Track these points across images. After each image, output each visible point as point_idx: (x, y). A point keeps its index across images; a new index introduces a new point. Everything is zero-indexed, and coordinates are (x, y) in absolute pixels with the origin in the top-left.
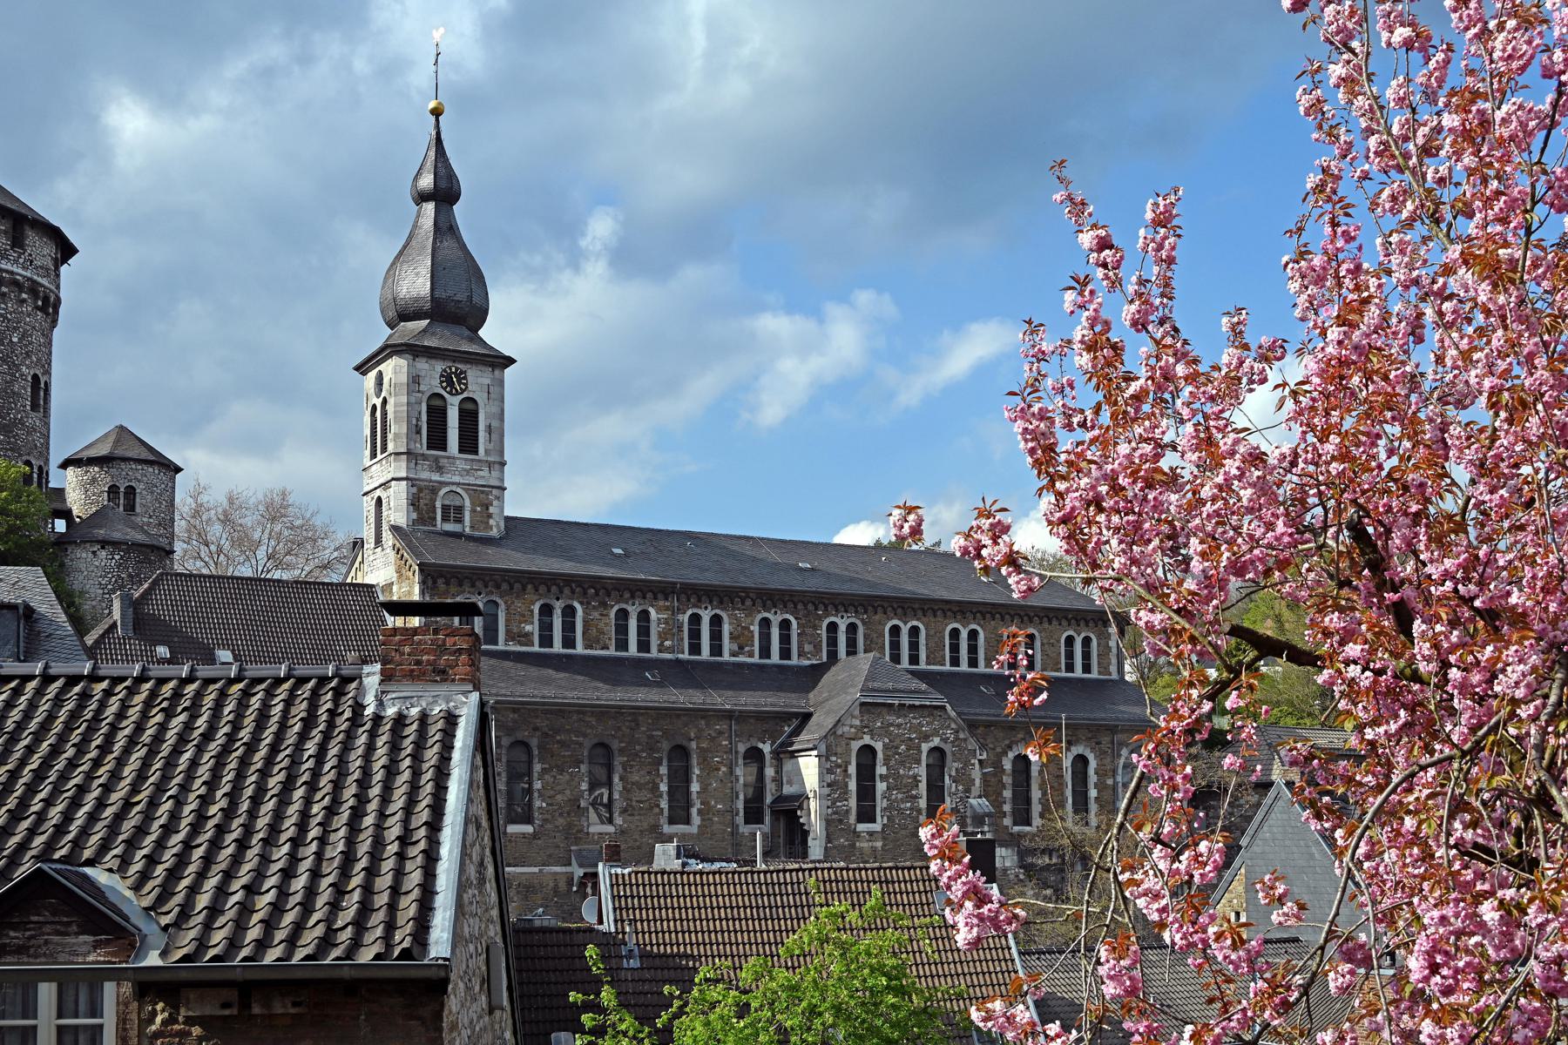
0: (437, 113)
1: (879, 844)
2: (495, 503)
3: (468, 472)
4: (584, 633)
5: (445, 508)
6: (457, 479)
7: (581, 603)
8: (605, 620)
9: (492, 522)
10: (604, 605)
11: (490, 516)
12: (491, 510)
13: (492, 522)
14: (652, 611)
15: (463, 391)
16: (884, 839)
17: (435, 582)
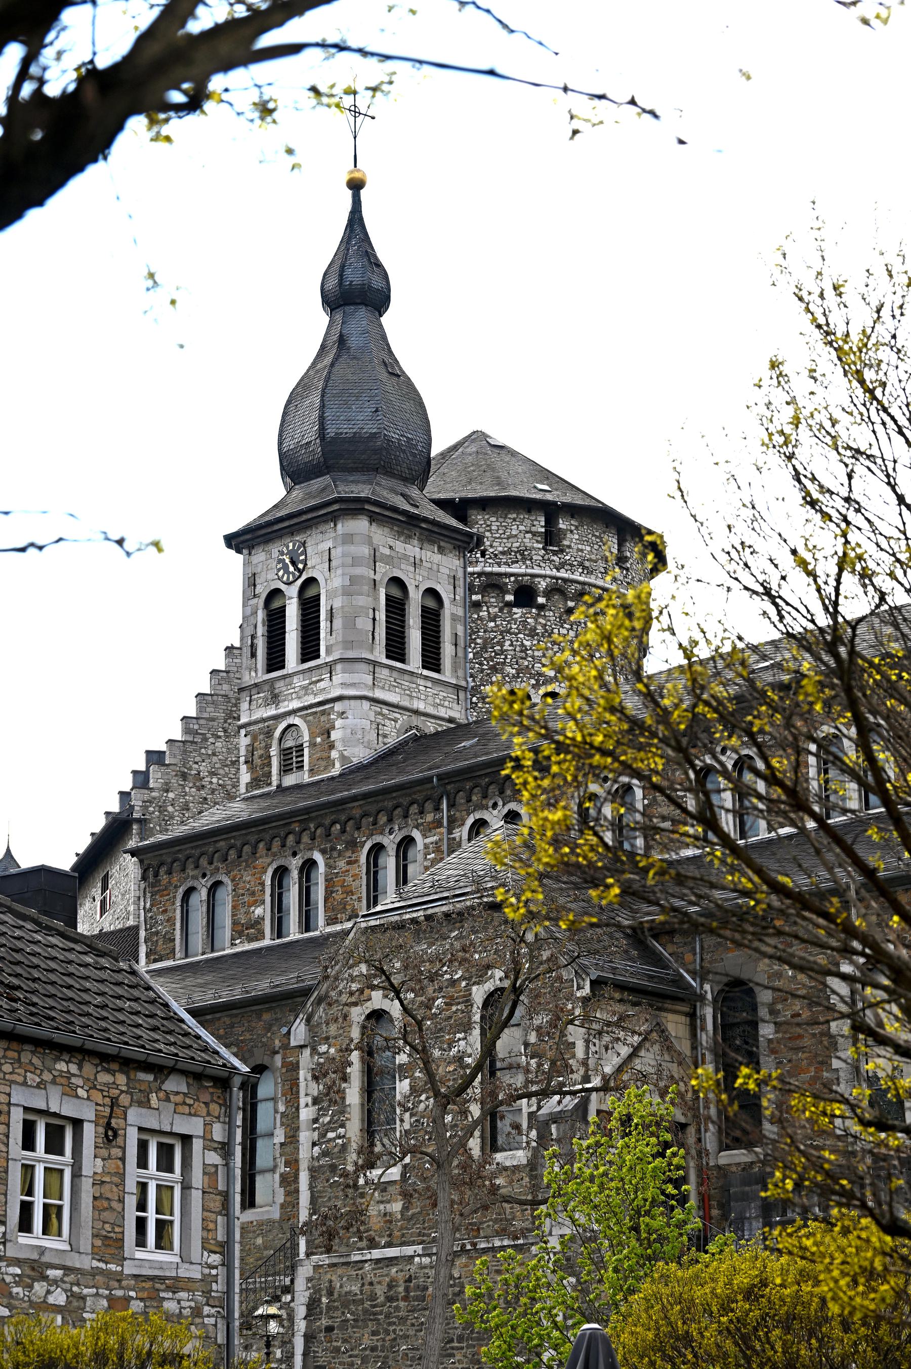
0: (356, 186)
1: (397, 1207)
2: (338, 723)
3: (305, 688)
4: (326, 900)
5: (285, 754)
6: (295, 704)
7: (323, 852)
8: (354, 869)
9: (334, 754)
10: (354, 845)
11: (332, 746)
12: (334, 735)
13: (334, 754)
14: (416, 834)
15: (301, 572)
16: (407, 1196)
17: (156, 875)
